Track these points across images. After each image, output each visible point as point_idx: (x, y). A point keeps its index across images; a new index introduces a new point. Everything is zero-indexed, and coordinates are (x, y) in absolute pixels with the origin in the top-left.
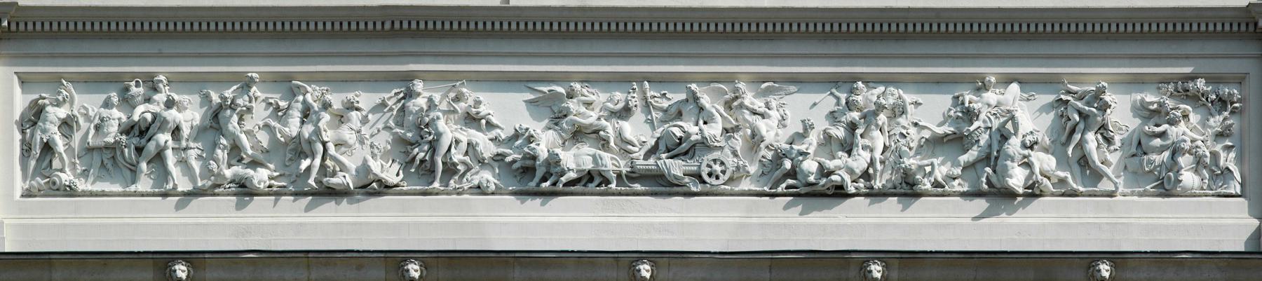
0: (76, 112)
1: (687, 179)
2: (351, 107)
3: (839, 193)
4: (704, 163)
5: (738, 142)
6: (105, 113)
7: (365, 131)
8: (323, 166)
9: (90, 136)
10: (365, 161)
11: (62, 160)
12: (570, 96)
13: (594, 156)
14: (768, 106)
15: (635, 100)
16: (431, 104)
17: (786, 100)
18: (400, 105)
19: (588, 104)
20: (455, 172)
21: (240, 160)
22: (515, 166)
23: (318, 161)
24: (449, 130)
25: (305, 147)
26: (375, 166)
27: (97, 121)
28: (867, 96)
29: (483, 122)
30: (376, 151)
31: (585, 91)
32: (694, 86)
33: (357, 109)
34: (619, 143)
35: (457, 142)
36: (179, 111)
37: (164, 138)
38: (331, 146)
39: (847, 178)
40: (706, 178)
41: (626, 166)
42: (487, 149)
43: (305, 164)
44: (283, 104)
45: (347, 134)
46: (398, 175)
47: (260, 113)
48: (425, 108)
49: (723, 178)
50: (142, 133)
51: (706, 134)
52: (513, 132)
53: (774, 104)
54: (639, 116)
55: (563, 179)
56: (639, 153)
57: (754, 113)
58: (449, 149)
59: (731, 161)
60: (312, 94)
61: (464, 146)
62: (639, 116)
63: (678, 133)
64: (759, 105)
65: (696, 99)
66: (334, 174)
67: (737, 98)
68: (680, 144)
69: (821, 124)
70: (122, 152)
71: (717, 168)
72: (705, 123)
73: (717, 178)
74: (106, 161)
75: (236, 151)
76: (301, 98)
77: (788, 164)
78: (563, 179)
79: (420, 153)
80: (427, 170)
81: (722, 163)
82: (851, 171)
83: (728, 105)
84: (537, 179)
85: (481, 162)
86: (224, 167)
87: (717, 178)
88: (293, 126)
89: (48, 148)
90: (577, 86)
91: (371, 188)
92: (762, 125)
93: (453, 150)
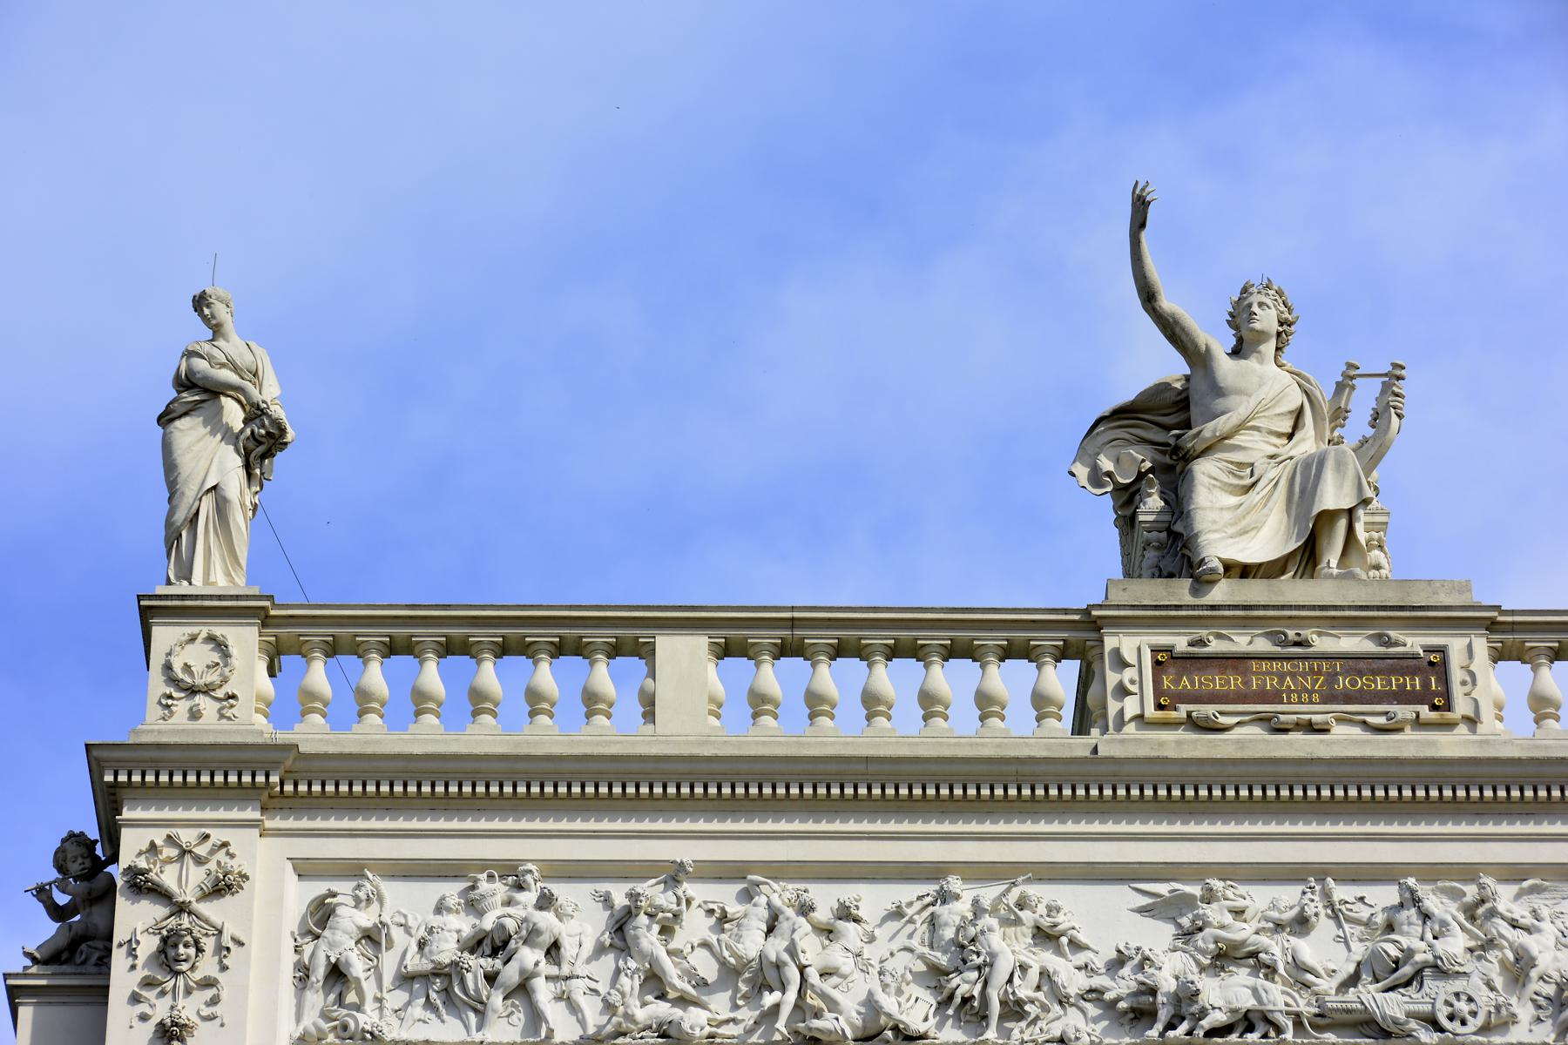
0: (386, 918)
1: (1413, 1024)
2: (846, 913)
4: (1437, 991)
5: (1492, 967)
6: (436, 921)
7: (872, 953)
8: (800, 1007)
9: (409, 957)
10: (870, 993)
11: (360, 993)
12: (1209, 897)
13: (1255, 991)
14: (1535, 914)
15: (1315, 906)
16: (978, 909)
18: (926, 914)
19: (1238, 913)
21: (662, 996)
22: (1122, 1005)
23: (791, 995)
24: (1008, 948)
25: (771, 976)
26: (888, 1003)
27: (422, 933)
29: (1064, 940)
30: (888, 979)
31: (1229, 894)
32: (1411, 881)
33: (857, 920)
34: (1294, 972)
35: (1024, 968)
36: (560, 917)
37: (529, 956)
38: (813, 976)
40: (1445, 1023)
41: (1309, 1004)
42: (1074, 982)
43: (769, 999)
44: (733, 909)
45: (837, 956)
46: (926, 1019)
47: (696, 925)
48: (970, 916)
49: (1474, 1024)
50: (494, 953)
51: (1440, 952)
52: (1114, 954)
53: (1545, 912)
54: (1324, 927)
55: (1206, 1023)
56: (1327, 985)
57: (1514, 925)
58: (1010, 981)
59: (1484, 997)
60: (780, 894)
61: (1033, 975)
62: (1324, 927)
63: (1394, 952)
64: (1521, 912)
65: (1416, 901)
66: (817, 1015)
67: (1483, 901)
68: (1396, 970)
70: (462, 981)
71: (1463, 1007)
72: (1435, 938)
73: (1463, 1023)
74: (433, 995)
75: (655, 983)
76: (762, 900)
78: (1206, 1023)
79: (965, 984)
80: (972, 1012)
81: (1470, 1000)
83: (1470, 912)
84: (1159, 1026)
85: (1063, 1001)
86: (634, 1003)
87: (1463, 1023)
88: (752, 943)
89: (337, 974)
90: (1217, 884)
92: (1531, 943)
93: (1016, 980)
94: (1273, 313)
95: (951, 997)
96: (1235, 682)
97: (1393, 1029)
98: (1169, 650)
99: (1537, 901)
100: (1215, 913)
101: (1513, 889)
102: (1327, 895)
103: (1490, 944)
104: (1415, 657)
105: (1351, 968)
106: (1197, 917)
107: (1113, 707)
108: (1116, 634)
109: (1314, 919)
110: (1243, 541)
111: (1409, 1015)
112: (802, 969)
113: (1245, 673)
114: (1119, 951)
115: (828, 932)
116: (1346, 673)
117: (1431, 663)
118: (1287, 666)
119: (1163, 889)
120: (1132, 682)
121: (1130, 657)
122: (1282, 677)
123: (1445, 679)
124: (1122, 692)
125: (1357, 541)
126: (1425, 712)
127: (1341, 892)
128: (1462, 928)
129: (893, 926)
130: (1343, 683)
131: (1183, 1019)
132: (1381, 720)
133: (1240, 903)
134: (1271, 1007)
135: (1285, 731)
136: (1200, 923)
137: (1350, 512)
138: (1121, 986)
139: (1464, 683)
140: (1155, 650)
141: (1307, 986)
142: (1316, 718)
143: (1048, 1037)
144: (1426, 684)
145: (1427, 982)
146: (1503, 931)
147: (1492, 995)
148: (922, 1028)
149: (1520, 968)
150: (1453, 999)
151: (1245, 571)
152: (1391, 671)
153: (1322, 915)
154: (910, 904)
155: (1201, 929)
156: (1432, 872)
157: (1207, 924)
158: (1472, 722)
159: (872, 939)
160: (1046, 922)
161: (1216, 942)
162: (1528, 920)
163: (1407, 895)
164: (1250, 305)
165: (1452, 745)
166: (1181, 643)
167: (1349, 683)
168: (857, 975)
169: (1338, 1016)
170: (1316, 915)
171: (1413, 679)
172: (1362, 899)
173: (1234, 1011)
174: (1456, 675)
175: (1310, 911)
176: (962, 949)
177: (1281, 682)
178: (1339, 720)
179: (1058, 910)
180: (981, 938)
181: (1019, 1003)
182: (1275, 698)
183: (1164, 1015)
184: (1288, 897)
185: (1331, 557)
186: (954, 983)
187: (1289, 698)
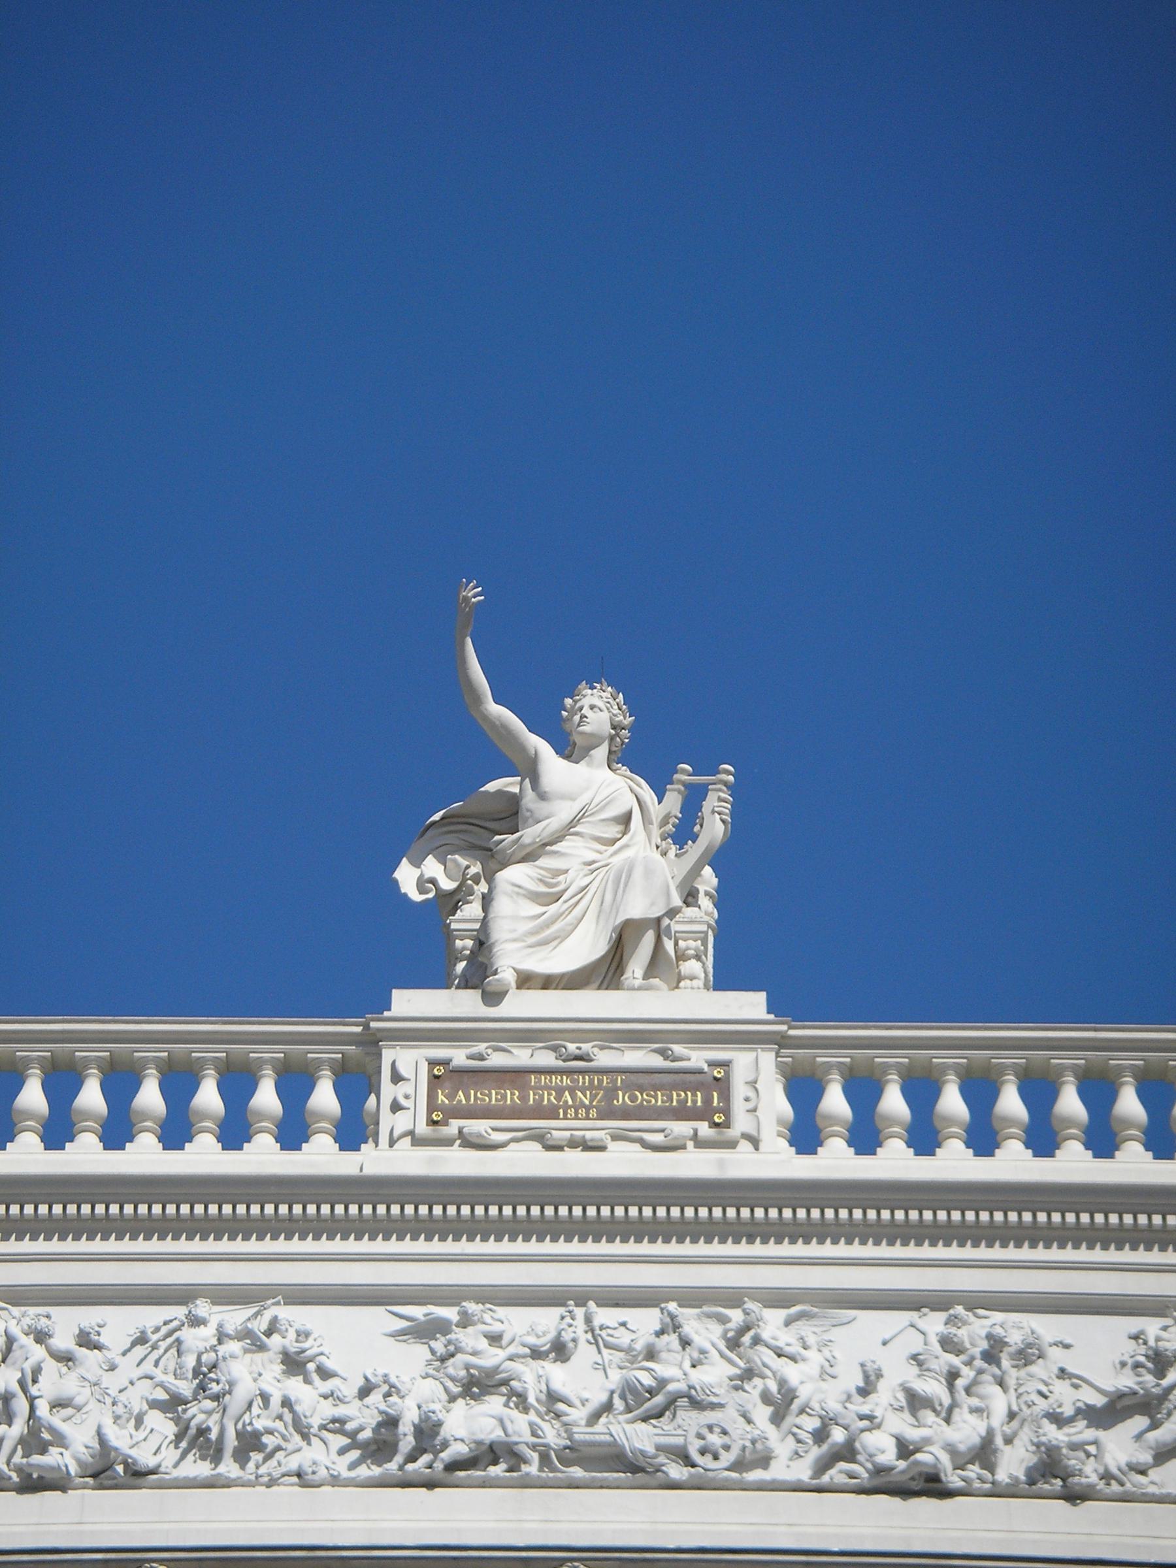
1: (662, 1459)
2: (86, 1340)
3: (931, 1486)
4: (686, 1426)
7: (112, 1382)
12: (466, 1321)
13: (501, 1421)
16: (222, 1336)
17: (836, 1334)
19: (495, 1339)
20: (260, 1447)
23: (18, 1428)
24: (250, 1374)
26: (119, 1438)
28: (976, 1329)
29: (311, 1366)
31: (487, 1317)
33: (97, 1347)
35: (265, 1398)
38: (43, 1409)
39: (945, 1460)
49: (727, 1458)
53: (811, 1340)
54: (584, 1354)
56: (577, 1415)
59: (738, 1427)
61: (275, 1401)
63: (647, 1380)
64: (786, 1338)
65: (676, 1327)
69: (897, 1373)
71: (715, 1439)
73: (716, 1457)
77: (838, 1435)
79: (198, 1413)
81: (725, 1432)
82: (951, 1450)
84: (399, 1459)
87: (716, 1457)
90: (472, 1307)
91: (109, 1471)
92: (793, 1373)
93: (255, 1410)
94: (605, 716)
95: (187, 1428)
96: (512, 1097)
97: (641, 1462)
98: (445, 1063)
99: (805, 1328)
100: (470, 1338)
101: (780, 1315)
102: (588, 1320)
103: (749, 1374)
104: (700, 1072)
105: (604, 1397)
106: (449, 1342)
107: (388, 1122)
108: (394, 1047)
109: (571, 1345)
110: (544, 951)
111: (660, 1448)
112: (32, 1400)
113: (524, 1089)
114: (366, 1379)
115: (66, 1359)
116: (627, 1087)
117: (716, 1079)
118: (566, 1081)
119: (417, 1312)
120: (407, 1097)
121: (403, 1070)
122: (560, 1092)
123: (726, 1096)
124: (396, 1107)
125: (666, 953)
126: (704, 1129)
127: (605, 1316)
128: (722, 1355)
129: (140, 1351)
130: (622, 1098)
131: (425, 1451)
132: (657, 1138)
133: (497, 1327)
134: (515, 1439)
135: (559, 1148)
136: (452, 1348)
137: (658, 920)
138: (364, 1417)
139: (747, 1099)
140: (432, 1063)
141: (558, 1416)
142: (589, 1135)
143: (283, 1469)
144: (708, 1100)
145: (680, 1413)
146: (766, 1360)
147: (748, 1428)
148: (150, 1461)
149: (782, 1404)
150: (705, 1431)
151: (548, 982)
152: (675, 1087)
153: (582, 1343)
154: (157, 1330)
155: (453, 1355)
156: (693, 1298)
157: (458, 1350)
158: (755, 1142)
159: (113, 1368)
160: (293, 1348)
161: (468, 1370)
162: (795, 1349)
163: (668, 1320)
164: (581, 709)
165: (742, 1165)
166: (459, 1056)
167: (627, 1100)
168: (93, 1405)
169: (586, 1451)
170: (574, 1340)
171: (694, 1095)
172: (624, 1324)
173: (479, 1443)
174: (739, 1090)
175: (567, 1336)
176: (203, 1375)
177: (558, 1098)
178: (615, 1138)
179: (307, 1335)
180: (222, 1364)
181: (257, 1435)
182: (551, 1113)
183: (407, 1443)
184: (543, 1322)
185: (635, 969)
186: (190, 1413)
187: (565, 1113)
